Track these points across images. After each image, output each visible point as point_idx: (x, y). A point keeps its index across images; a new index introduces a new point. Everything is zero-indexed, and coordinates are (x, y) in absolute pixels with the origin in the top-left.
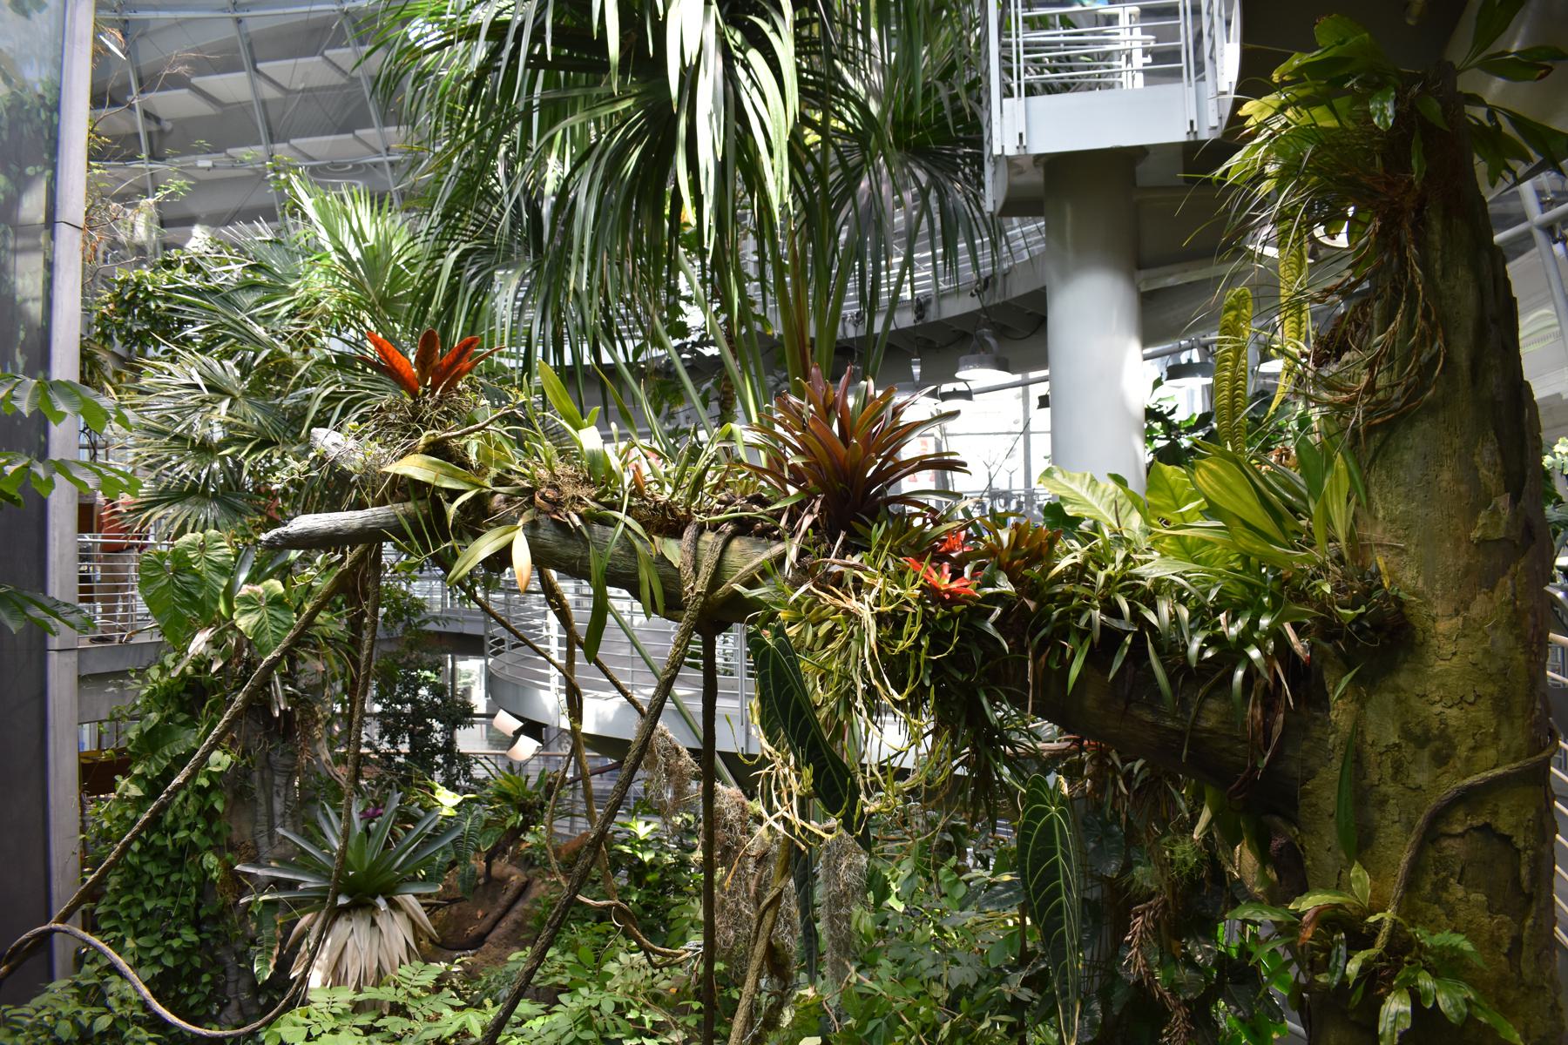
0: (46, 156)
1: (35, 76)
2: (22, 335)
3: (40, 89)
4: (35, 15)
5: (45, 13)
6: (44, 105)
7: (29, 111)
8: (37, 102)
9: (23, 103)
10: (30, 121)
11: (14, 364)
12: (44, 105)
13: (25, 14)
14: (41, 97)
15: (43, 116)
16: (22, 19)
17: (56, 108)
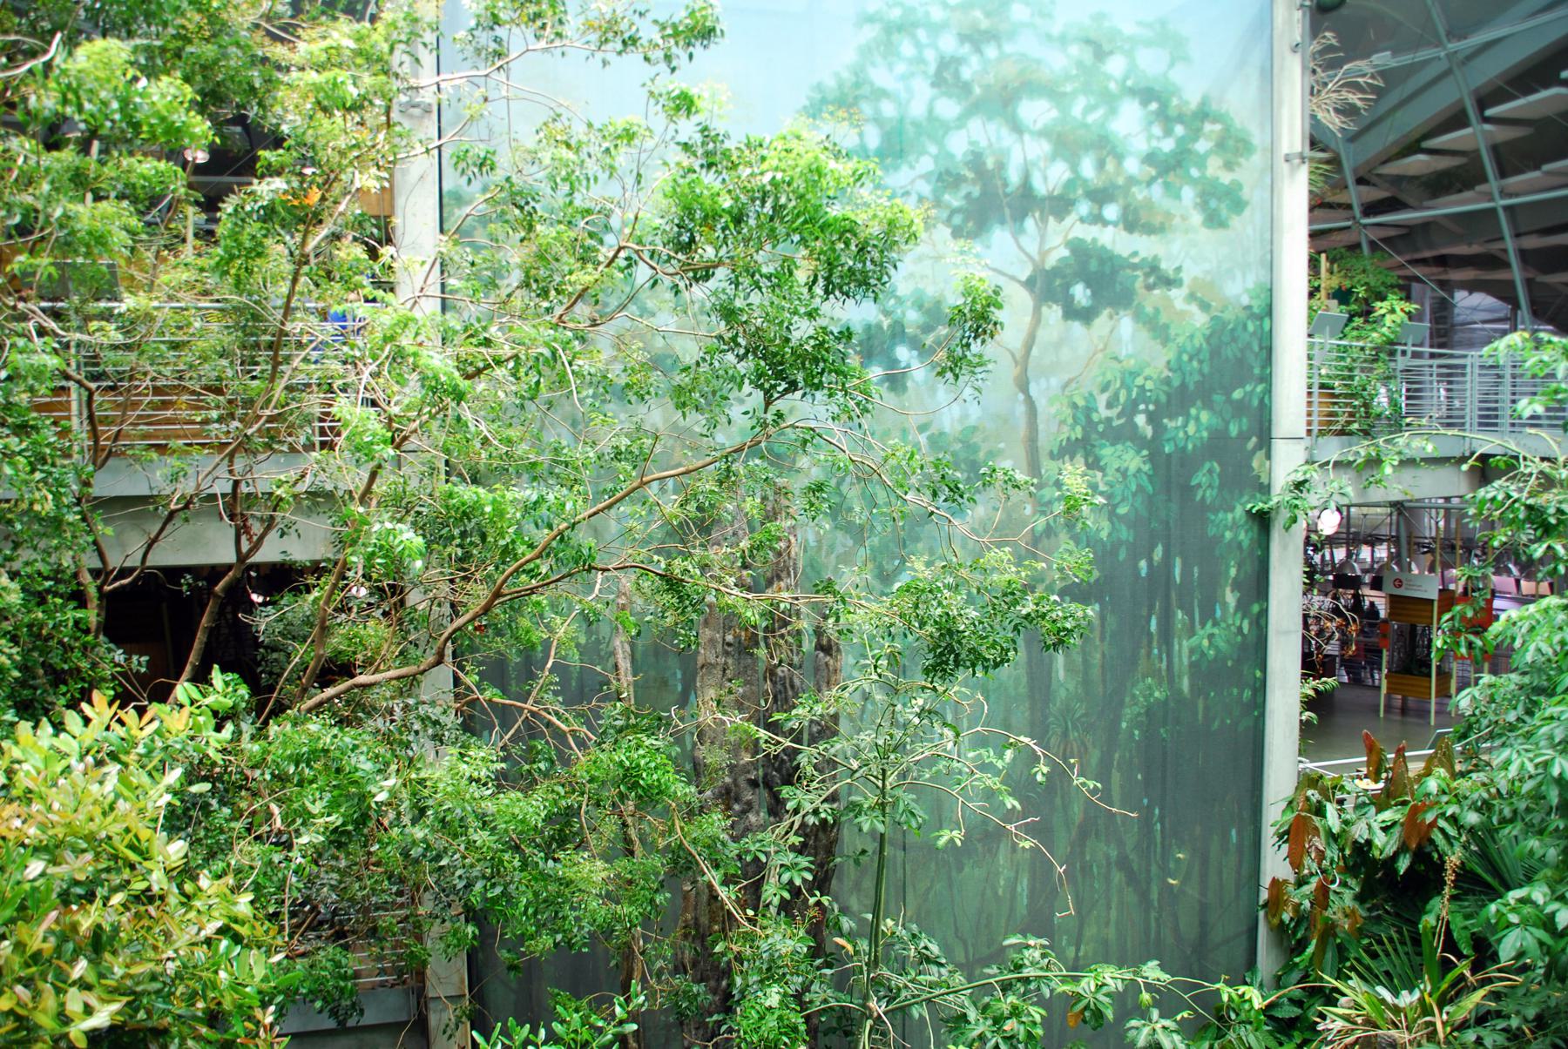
0: (1257, 371)
1: (1239, 290)
2: (1233, 572)
3: (1245, 300)
4: (1235, 221)
5: (1247, 212)
6: (1253, 316)
7: (1233, 330)
8: (1243, 315)
9: (1224, 324)
10: (1234, 339)
11: (1225, 605)
12: (1253, 316)
13: (1222, 225)
14: (1248, 308)
15: (1251, 327)
16: (1220, 234)
17: (1269, 311)
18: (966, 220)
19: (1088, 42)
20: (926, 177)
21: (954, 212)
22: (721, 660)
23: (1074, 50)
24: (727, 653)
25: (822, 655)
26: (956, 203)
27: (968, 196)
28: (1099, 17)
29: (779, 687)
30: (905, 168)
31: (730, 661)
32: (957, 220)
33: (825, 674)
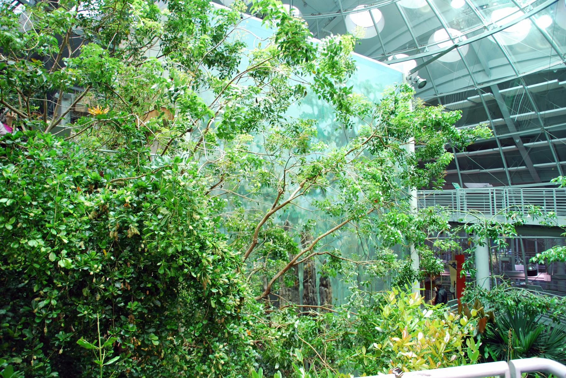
18: (339, 141)
19: (365, 88)
20: (329, 125)
21: (337, 138)
22: (287, 293)
23: (363, 90)
24: (289, 290)
25: (323, 288)
26: (337, 135)
27: (340, 133)
28: (368, 81)
29: (310, 301)
30: (324, 122)
31: (290, 293)
32: (337, 140)
33: (325, 294)
